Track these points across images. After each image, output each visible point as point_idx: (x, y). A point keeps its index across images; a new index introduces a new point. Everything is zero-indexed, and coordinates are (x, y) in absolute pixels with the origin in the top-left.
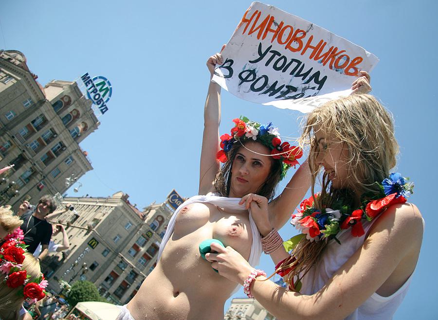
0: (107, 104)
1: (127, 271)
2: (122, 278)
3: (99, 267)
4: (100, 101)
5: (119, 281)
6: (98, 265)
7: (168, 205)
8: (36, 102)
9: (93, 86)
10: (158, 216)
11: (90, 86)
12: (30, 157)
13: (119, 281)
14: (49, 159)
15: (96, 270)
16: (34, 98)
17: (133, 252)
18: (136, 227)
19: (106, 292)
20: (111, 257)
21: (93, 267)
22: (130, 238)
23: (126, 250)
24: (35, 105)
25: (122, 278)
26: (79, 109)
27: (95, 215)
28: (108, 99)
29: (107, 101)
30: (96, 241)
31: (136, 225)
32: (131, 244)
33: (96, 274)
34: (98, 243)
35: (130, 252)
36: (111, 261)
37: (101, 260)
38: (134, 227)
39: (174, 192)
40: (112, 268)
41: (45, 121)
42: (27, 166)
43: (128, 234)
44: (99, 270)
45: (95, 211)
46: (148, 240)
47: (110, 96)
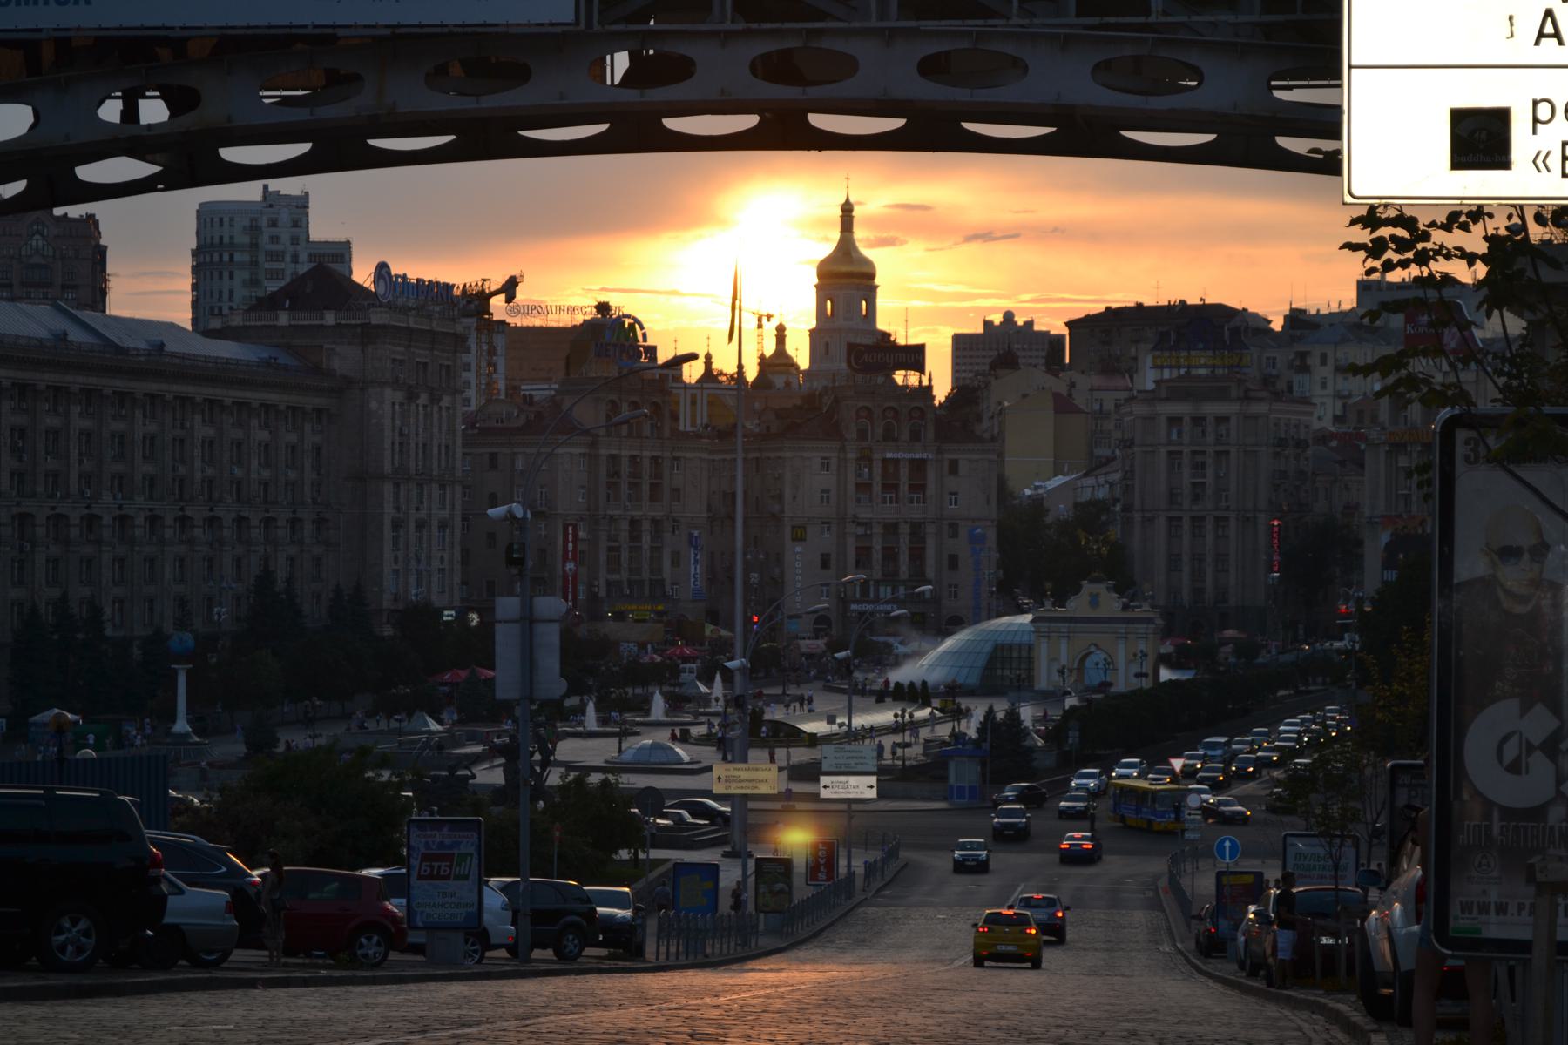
0: (650, 342)
1: (878, 530)
2: (877, 545)
5: (877, 556)
7: (859, 377)
9: (615, 345)
13: (877, 556)
14: (655, 488)
21: (825, 564)
28: (644, 335)
29: (645, 339)
32: (851, 487)
35: (858, 500)
39: (851, 347)
41: (614, 458)
42: (646, 526)
46: (870, 460)
47: (642, 328)
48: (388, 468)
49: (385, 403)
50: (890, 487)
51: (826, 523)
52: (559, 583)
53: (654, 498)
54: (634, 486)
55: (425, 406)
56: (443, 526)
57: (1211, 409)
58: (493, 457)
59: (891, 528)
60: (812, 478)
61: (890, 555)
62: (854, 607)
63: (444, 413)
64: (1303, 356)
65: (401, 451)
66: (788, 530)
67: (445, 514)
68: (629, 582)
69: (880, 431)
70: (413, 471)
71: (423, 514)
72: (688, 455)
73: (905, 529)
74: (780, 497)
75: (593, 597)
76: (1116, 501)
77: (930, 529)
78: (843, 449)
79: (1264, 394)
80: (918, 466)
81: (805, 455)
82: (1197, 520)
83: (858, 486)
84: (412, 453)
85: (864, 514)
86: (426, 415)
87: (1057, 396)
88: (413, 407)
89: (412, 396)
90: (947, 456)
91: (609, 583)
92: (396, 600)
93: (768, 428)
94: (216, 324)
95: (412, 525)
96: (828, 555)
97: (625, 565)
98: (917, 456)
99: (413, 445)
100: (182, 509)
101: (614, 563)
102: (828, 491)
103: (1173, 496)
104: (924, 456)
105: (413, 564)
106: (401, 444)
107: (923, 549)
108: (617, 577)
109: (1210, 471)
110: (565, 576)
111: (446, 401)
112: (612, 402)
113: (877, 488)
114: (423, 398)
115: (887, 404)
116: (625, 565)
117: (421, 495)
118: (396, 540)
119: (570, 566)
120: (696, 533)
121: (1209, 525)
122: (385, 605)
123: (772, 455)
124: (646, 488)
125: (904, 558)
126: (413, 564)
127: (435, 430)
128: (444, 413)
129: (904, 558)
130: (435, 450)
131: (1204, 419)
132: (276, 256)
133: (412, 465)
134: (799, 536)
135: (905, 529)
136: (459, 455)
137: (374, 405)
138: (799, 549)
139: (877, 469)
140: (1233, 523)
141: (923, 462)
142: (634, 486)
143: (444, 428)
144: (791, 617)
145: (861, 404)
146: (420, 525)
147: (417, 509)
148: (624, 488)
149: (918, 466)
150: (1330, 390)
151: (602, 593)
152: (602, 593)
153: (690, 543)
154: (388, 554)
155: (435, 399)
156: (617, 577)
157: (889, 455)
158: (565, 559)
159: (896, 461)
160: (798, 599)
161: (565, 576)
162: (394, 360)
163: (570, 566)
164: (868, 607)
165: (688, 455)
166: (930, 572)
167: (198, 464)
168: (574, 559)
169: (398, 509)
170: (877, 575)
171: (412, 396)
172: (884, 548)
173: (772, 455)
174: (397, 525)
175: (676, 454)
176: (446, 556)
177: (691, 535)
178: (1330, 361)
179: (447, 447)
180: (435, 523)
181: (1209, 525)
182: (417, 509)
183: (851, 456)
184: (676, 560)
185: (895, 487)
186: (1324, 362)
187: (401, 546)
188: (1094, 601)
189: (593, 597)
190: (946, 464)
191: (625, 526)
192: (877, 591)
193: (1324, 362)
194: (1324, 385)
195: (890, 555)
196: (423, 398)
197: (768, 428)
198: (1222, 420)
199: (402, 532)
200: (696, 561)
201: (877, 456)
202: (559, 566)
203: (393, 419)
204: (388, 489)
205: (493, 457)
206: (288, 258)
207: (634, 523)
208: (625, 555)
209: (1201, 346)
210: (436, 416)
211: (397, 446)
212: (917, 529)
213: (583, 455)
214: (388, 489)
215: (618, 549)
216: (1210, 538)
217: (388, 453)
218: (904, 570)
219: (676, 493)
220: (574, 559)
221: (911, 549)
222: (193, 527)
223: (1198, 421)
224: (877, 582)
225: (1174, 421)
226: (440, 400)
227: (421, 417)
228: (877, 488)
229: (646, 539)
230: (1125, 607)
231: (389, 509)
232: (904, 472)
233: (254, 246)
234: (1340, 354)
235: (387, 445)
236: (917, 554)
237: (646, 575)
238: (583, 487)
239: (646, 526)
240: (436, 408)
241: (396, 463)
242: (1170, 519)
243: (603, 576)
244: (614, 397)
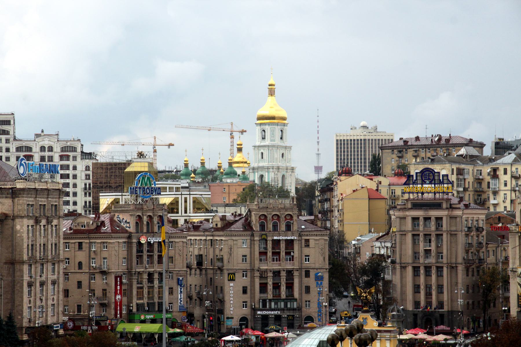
1: (270, 274)
2: (270, 282)
3: (249, 288)
4: (152, 190)
5: (270, 287)
6: (246, 287)
8: (127, 240)
9: (140, 188)
10: (260, 217)
11: (138, 190)
12: (153, 270)
13: (270, 287)
14: (160, 257)
15: (249, 291)
16: (124, 240)
17: (263, 258)
18: (251, 239)
19: (268, 301)
20: (251, 275)
21: (245, 291)
22: (252, 251)
23: (257, 262)
24: (128, 242)
25: (270, 282)
26: (148, 214)
27: (214, 252)
30: (232, 274)
31: (249, 238)
33: (251, 293)
34: (234, 274)
35: (261, 260)
36: (253, 278)
37: (245, 281)
38: (249, 241)
40: (257, 281)
42: (156, 276)
43: (249, 249)
44: (251, 290)
45: (211, 246)
46: (266, 240)
48: (25, 258)
49: (22, 227)
50: (277, 254)
51: (245, 271)
52: (113, 306)
53: (160, 261)
54: (150, 257)
55: (44, 226)
56: (54, 283)
57: (434, 213)
58: (80, 244)
59: (277, 274)
60: (238, 250)
61: (277, 286)
62: (259, 313)
63: (54, 228)
64: (495, 170)
65: (32, 249)
66: (226, 276)
67: (55, 277)
68: (148, 303)
69: (270, 226)
70: (38, 258)
71: (43, 278)
72: (177, 240)
73: (283, 274)
74: (221, 260)
75: (130, 311)
76: (389, 257)
77: (296, 274)
78: (253, 235)
80: (290, 243)
81: (234, 238)
82: (428, 269)
83: (261, 253)
84: (38, 249)
85: (264, 267)
86: (45, 230)
87: (369, 190)
88: (38, 227)
89: (37, 221)
91: (137, 305)
92: (30, 322)
93: (217, 225)
95: (38, 284)
96: (246, 287)
97: (146, 295)
98: (289, 238)
99: (38, 245)
101: (140, 296)
102: (246, 256)
103: (416, 255)
104: (292, 238)
105: (38, 303)
106: (32, 245)
107: (293, 284)
108: (141, 301)
109: (433, 244)
110: (116, 302)
111: (55, 222)
112: (139, 216)
113: (270, 254)
114: (43, 222)
116: (146, 295)
117: (43, 269)
119: (118, 297)
120: (181, 278)
121: (434, 271)
122: (25, 324)
123: (218, 238)
124: (156, 257)
125: (283, 288)
126: (38, 303)
127: (50, 237)
128: (54, 228)
129: (283, 288)
130: (50, 247)
131: (430, 218)
133: (38, 254)
134: (232, 280)
135: (283, 274)
136: (61, 248)
137: (18, 227)
138: (232, 284)
139: (270, 245)
140: (445, 269)
141: (292, 241)
142: (150, 257)
143: (54, 234)
144: (228, 318)
145: (261, 213)
146: (42, 284)
147: (41, 276)
148: (145, 257)
149: (290, 243)
150: (509, 187)
151: (135, 310)
152: (135, 310)
153: (178, 284)
155: (49, 222)
156: (141, 301)
157: (275, 238)
158: (116, 294)
159: (279, 240)
160: (232, 309)
161: (116, 302)
162: (28, 205)
163: (118, 297)
164: (265, 313)
165: (177, 240)
166: (296, 295)
168: (121, 293)
169: (31, 277)
170: (270, 295)
171: (37, 221)
172: (273, 284)
173: (218, 238)
174: (30, 285)
175: (171, 240)
176: (55, 297)
177: (178, 279)
178: (509, 172)
179: (56, 244)
180: (50, 282)
181: (434, 271)
182: (41, 276)
183: (257, 238)
184: (171, 291)
185: (279, 253)
186: (505, 173)
187: (33, 295)
189: (130, 311)
190: (303, 241)
191: (145, 276)
192: (270, 305)
193: (505, 173)
194: (506, 185)
195: (277, 286)
196: (43, 222)
197: (217, 225)
198: (439, 219)
199: (33, 288)
200: (181, 292)
201: (269, 238)
202: (114, 297)
203: (28, 233)
204: (26, 268)
205: (80, 244)
207: (150, 276)
208: (146, 291)
209: (428, 182)
210: (50, 230)
211: (30, 246)
212: (290, 273)
213: (125, 242)
214: (26, 268)
215: (142, 288)
216: (434, 277)
217: (25, 251)
218: (283, 294)
219: (171, 259)
220: (121, 293)
221: (286, 283)
223: (427, 219)
224: (270, 300)
225: (415, 219)
226: (51, 222)
227: (42, 231)
228: (270, 254)
229: (156, 283)
230: (380, 325)
231: (26, 278)
232: (283, 245)
234: (514, 169)
236: (290, 286)
237: (156, 300)
238: (125, 258)
239: (156, 276)
240: (50, 226)
241: (30, 254)
242: (414, 268)
243: (135, 301)
244: (140, 214)
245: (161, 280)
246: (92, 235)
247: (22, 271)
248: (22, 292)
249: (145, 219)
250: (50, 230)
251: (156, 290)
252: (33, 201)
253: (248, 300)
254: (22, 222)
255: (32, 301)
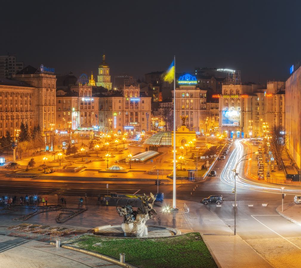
16: (76, 99)
26: (86, 90)
40: (125, 115)
48: (43, 104)
62: (125, 128)
67: (53, 112)
71: (49, 113)
77: (139, 113)
79: (199, 88)
89: (47, 90)
90: (142, 100)
94: (9, 77)
95: (48, 115)
100: (7, 114)
115: (131, 90)
118: (45, 118)
132: (11, 65)
137: (41, 92)
154: (44, 120)
164: (127, 128)
167: (9, 104)
168: (75, 119)
169: (45, 111)
188: (183, 129)
204: (43, 108)
206: (12, 65)
210: (51, 94)
217: (43, 101)
222: (9, 117)
229: (88, 115)
233: (7, 63)
235: (43, 100)
245: (90, 115)
246: (64, 98)
247: (42, 109)
248: (42, 118)
249: (84, 92)
250: (51, 94)
251: (88, 119)
252: (46, 82)
253: (121, 123)
254: (42, 90)
255: (46, 121)
